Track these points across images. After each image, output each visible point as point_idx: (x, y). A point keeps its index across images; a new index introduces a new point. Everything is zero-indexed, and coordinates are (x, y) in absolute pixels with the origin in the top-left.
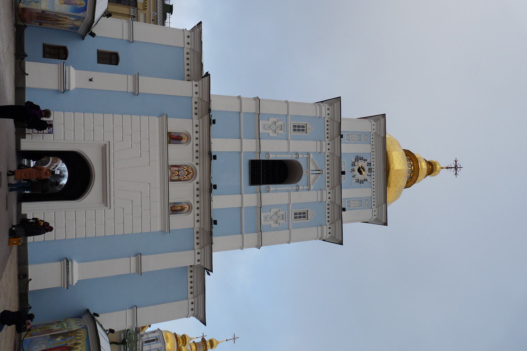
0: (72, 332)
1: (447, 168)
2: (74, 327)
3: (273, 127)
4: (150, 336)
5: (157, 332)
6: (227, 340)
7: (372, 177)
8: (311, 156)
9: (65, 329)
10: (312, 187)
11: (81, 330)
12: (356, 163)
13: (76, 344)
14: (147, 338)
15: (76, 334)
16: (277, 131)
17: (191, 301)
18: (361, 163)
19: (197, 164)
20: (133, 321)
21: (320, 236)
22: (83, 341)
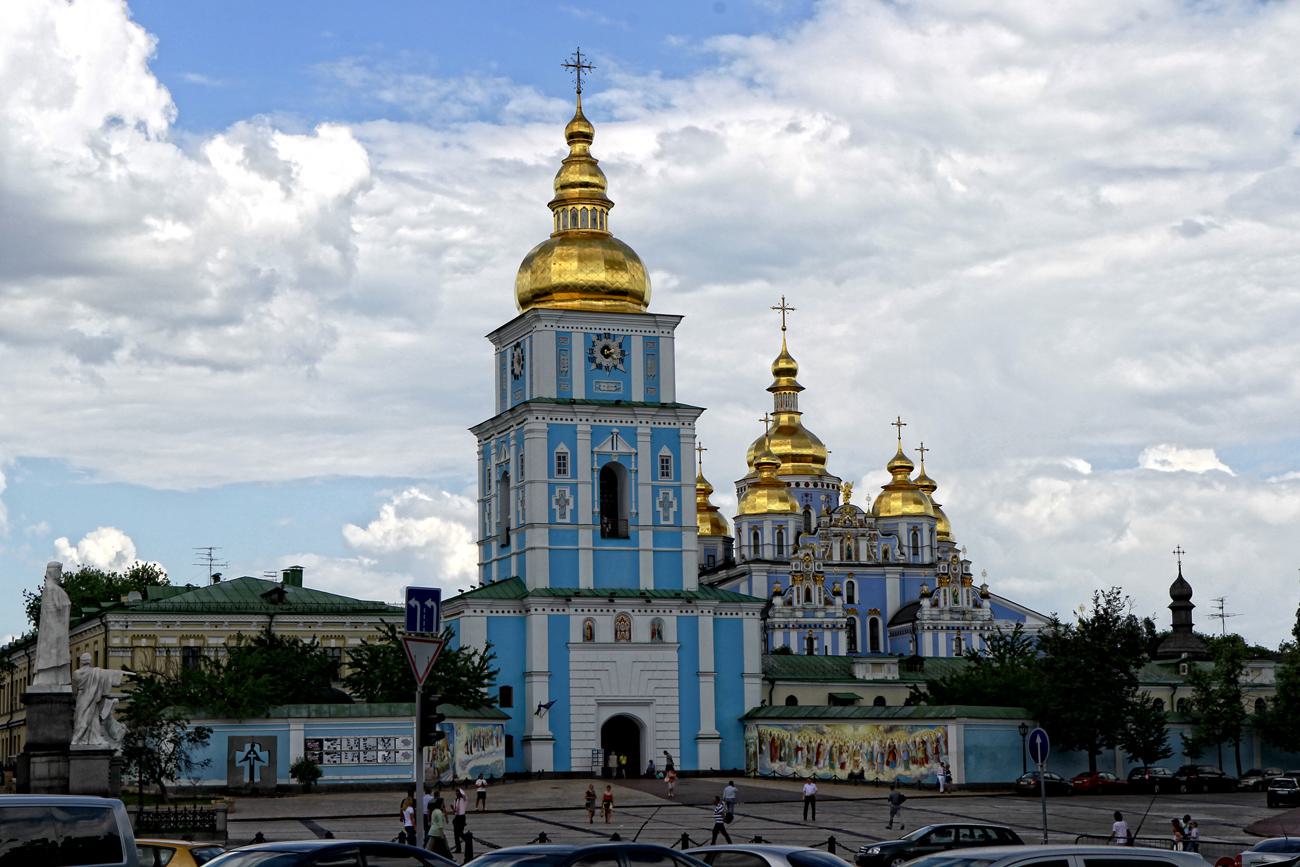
0: (760, 736)
1: (579, 93)
2: (756, 734)
3: (562, 502)
5: (741, 523)
6: (784, 330)
7: (616, 332)
8: (596, 449)
10: (634, 450)
12: (598, 361)
13: (771, 735)
14: (750, 549)
16: (567, 498)
17: (745, 616)
18: (597, 349)
19: (614, 611)
20: (754, 677)
21: (691, 440)
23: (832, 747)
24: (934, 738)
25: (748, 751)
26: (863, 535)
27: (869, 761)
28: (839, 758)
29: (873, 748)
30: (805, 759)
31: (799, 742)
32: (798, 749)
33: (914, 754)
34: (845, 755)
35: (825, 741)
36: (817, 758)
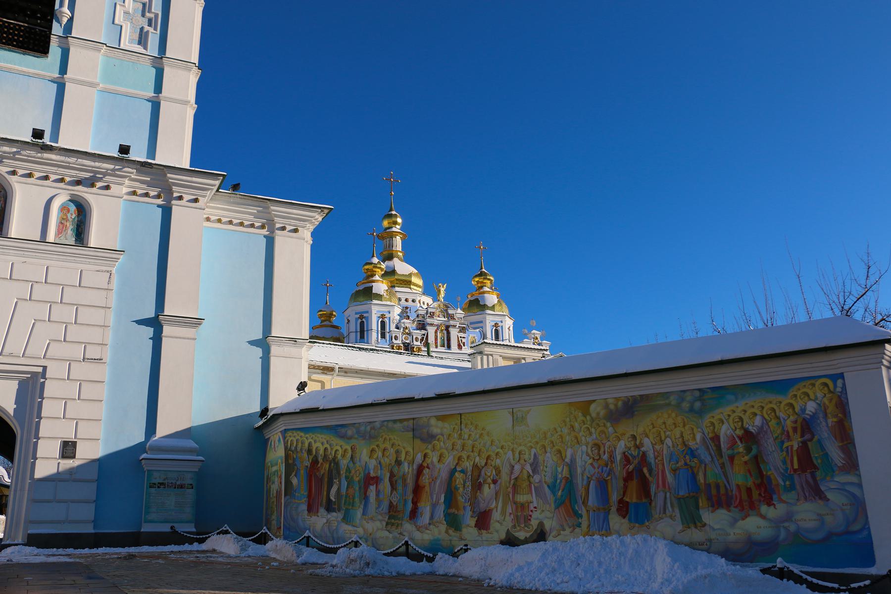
0: (287, 456)
4: (353, 328)
9: (280, 469)
11: (287, 441)
13: (309, 451)
15: (290, 450)
22: (307, 438)
23: (453, 472)
24: (789, 424)
25: (269, 491)
26: (454, 326)
27: (559, 504)
28: (473, 501)
29: (571, 466)
30: (385, 505)
31: (372, 463)
32: (370, 480)
33: (710, 475)
34: (488, 491)
35: (435, 460)
36: (415, 503)
